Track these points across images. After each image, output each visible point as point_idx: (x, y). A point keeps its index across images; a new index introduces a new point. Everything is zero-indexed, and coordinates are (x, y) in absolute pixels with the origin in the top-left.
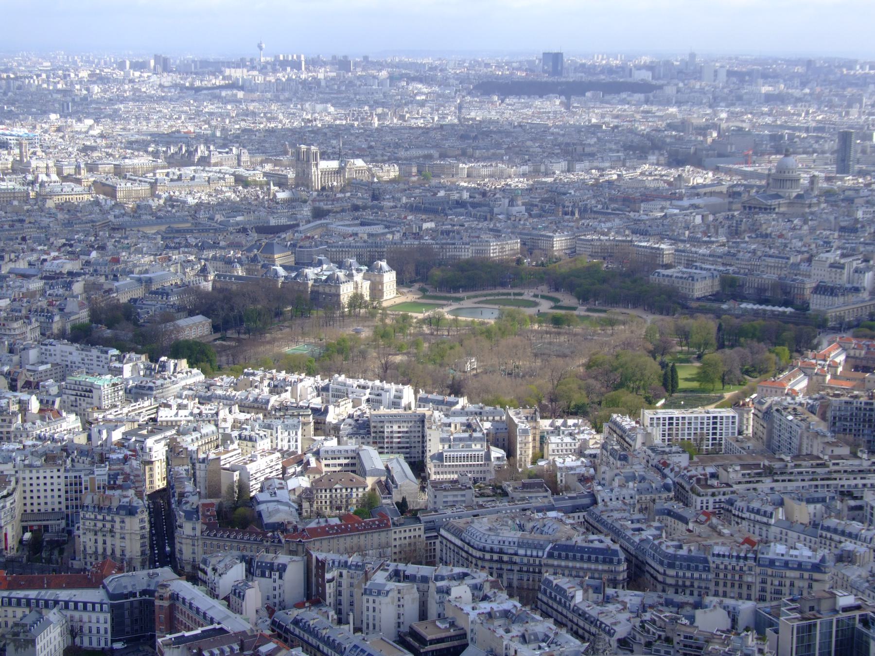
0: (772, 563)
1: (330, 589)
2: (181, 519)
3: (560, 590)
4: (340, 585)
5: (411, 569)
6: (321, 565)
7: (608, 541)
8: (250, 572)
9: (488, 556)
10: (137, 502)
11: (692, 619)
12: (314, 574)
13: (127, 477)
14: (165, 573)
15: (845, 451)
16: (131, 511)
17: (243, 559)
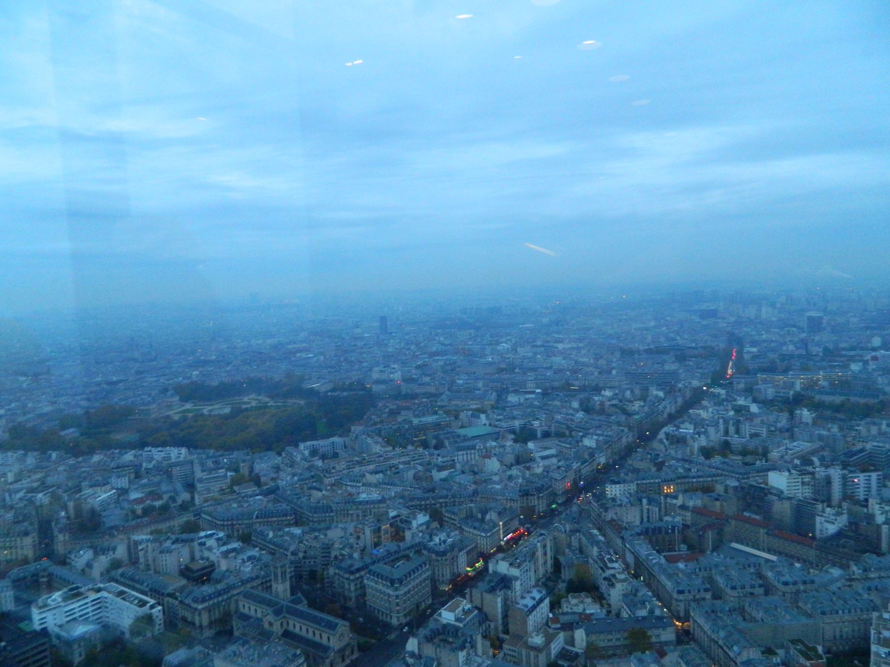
0: (360, 503)
1: (141, 554)
2: (56, 533)
3: (261, 533)
4: (147, 551)
5: (184, 536)
6: (137, 543)
7: (284, 506)
8: (96, 554)
9: (226, 523)
10: (30, 528)
11: (326, 535)
12: (132, 548)
13: (25, 515)
14: (45, 562)
15: (390, 448)
16: (26, 534)
17: (91, 547)
